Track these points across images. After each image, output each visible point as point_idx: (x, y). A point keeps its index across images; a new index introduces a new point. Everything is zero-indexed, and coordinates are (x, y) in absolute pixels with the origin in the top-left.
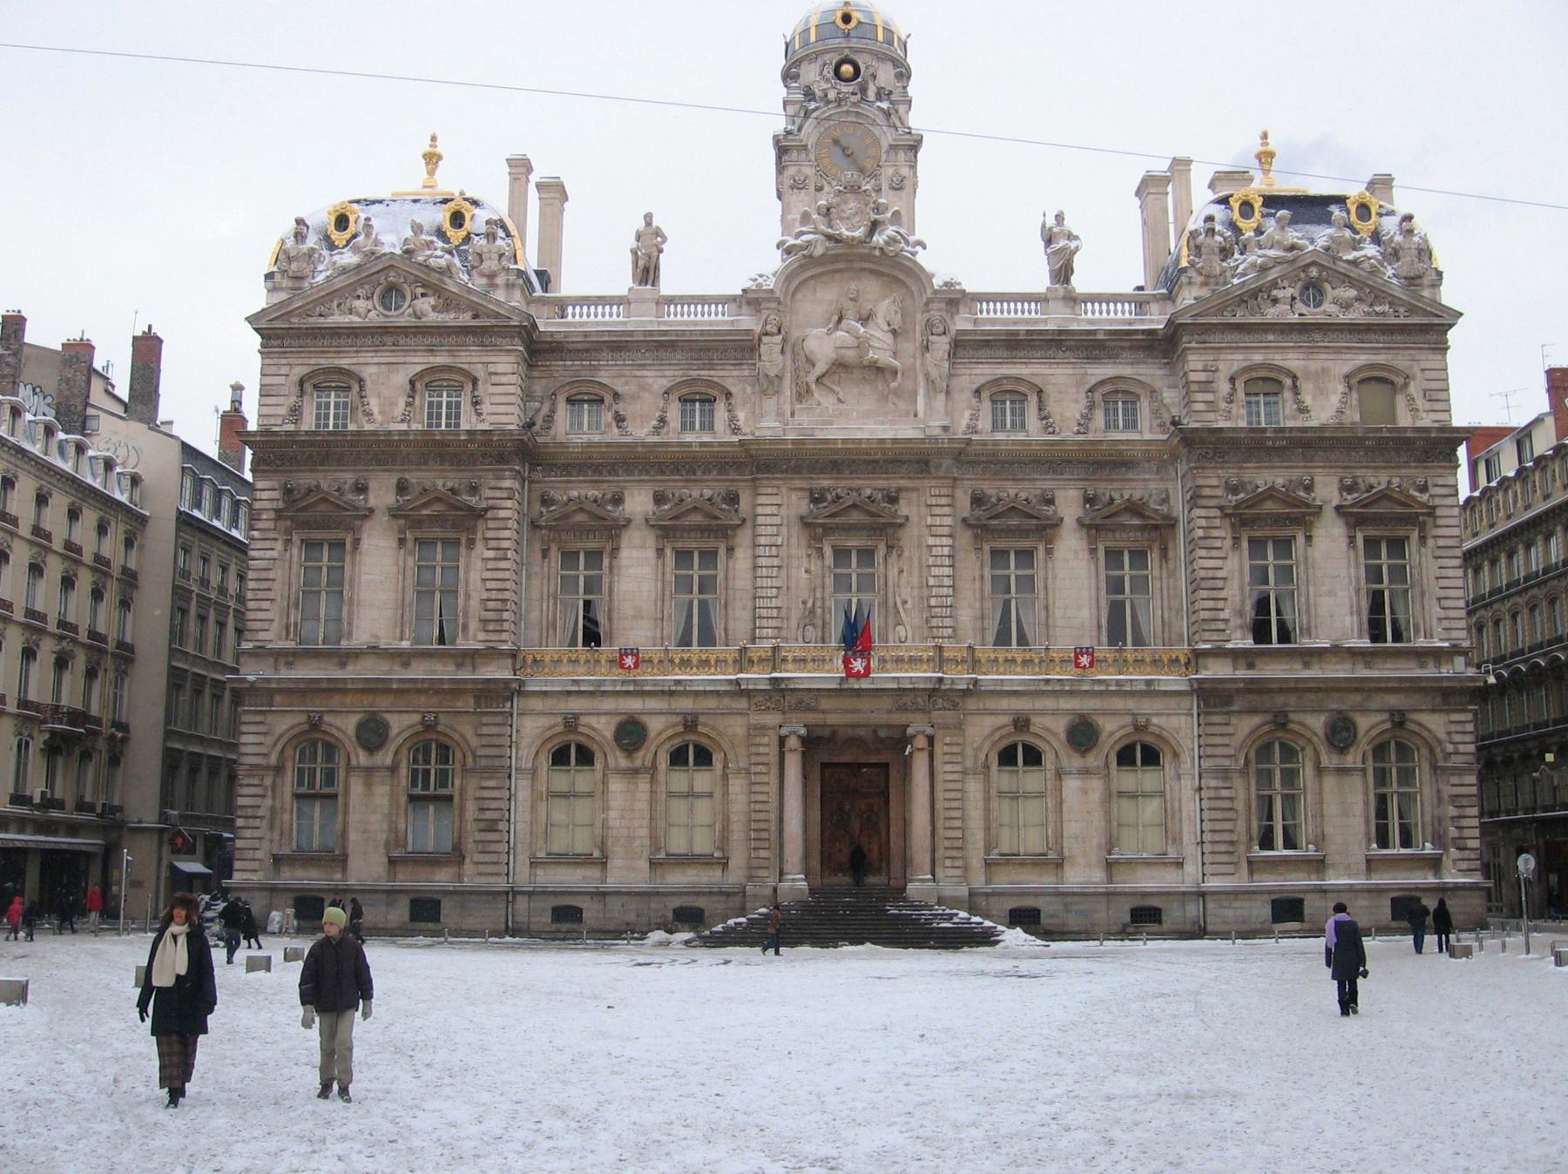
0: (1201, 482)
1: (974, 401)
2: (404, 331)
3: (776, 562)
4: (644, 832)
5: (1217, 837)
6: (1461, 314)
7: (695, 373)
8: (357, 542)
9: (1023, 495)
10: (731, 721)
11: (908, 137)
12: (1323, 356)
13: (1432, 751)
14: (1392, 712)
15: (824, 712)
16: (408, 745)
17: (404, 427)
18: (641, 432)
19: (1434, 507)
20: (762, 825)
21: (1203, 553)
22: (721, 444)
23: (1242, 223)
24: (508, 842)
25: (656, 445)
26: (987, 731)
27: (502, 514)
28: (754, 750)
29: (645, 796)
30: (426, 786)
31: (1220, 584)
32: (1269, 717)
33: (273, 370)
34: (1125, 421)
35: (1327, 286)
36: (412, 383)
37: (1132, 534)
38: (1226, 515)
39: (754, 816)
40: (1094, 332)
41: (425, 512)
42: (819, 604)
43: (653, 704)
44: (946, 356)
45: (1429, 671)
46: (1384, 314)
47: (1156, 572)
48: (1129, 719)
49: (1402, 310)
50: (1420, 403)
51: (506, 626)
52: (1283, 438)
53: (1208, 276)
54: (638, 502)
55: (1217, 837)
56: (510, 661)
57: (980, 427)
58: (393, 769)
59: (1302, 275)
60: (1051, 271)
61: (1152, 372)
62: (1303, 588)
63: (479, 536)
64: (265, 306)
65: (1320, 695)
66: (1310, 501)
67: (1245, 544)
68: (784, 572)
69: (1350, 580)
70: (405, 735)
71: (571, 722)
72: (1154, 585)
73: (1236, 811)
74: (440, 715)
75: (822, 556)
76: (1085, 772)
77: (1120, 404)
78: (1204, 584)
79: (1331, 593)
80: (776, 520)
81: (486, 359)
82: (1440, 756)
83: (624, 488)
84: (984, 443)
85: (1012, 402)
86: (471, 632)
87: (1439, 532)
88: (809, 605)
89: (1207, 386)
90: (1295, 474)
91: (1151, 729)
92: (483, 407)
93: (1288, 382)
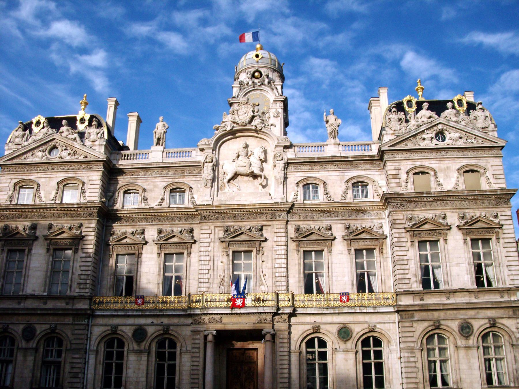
0: (395, 217)
1: (296, 188)
3: (208, 258)
4: (144, 379)
5: (409, 380)
7: (177, 180)
8: (30, 250)
9: (317, 227)
10: (184, 328)
11: (280, 97)
12: (447, 162)
13: (510, 336)
14: (489, 319)
15: (224, 324)
16: (44, 338)
17: (53, 202)
18: (154, 203)
19: (502, 225)
20: (196, 377)
21: (398, 249)
22: (185, 208)
24: (83, 383)
25: (158, 209)
26: (300, 333)
27: (90, 238)
28: (193, 341)
29: (145, 363)
30: (51, 357)
31: (406, 262)
32: (431, 323)
33: (4, 181)
34: (362, 195)
35: (446, 132)
36: (58, 184)
37: (366, 243)
38: (408, 231)
39: (192, 372)
40: (347, 157)
41: (58, 237)
42: (226, 276)
43: (149, 321)
44: (283, 169)
45: (506, 298)
47: (378, 259)
48: (366, 326)
49: (480, 141)
50: (492, 180)
51: (88, 286)
54: (151, 234)
55: (409, 380)
56: (88, 302)
57: (298, 199)
58: (36, 350)
62: (444, 264)
63: (80, 248)
65: (455, 312)
66: (445, 224)
67: (416, 244)
68: (211, 263)
69: (466, 258)
70: (42, 334)
71: (114, 329)
72: (377, 265)
73: (418, 368)
74: (58, 325)
75: (227, 253)
76: (346, 351)
77: (360, 187)
78: (399, 263)
79: (457, 264)
80: (209, 240)
81: (88, 175)
82: (514, 339)
83: (145, 228)
84: (299, 204)
85: (313, 188)
86: (73, 289)
87: (505, 236)
88: (222, 277)
89: (395, 176)
90: (438, 213)
91: (377, 330)
93: (432, 173)
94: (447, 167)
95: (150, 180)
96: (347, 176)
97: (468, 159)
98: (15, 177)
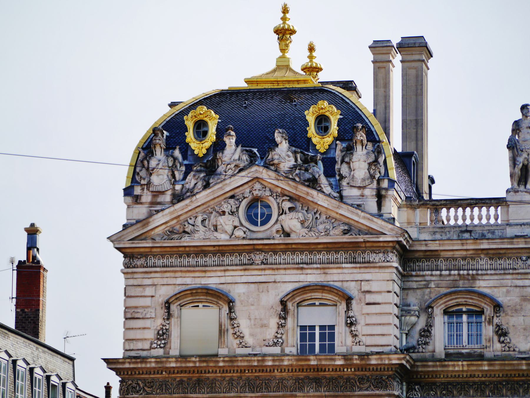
2: (274, 249)
17: (277, 350)
36: (283, 303)
64: (125, 222)
81: (359, 277)
92: (359, 327)
95: (509, 280)
98: (165, 281)
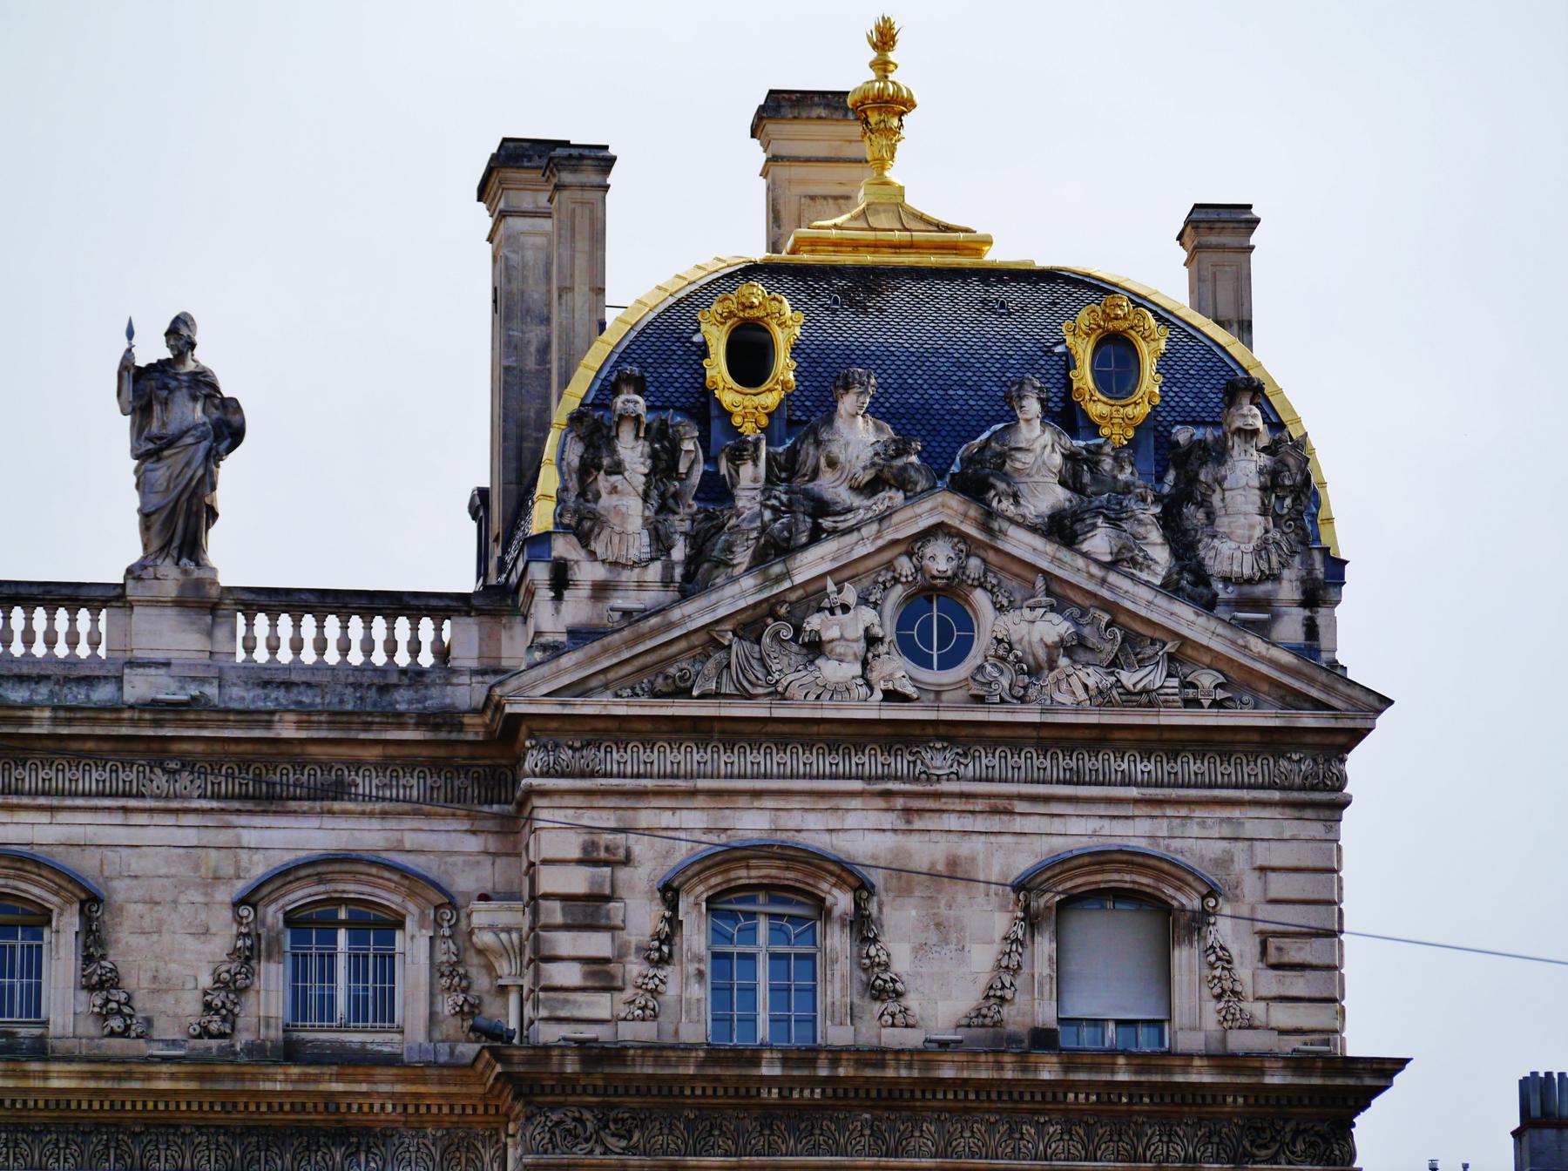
6: (1389, 702)
12: (952, 822)
23: (729, 394)
35: (980, 598)
40: (265, 717)
46: (1146, 698)
49: (1207, 680)
52: (814, 1081)
53: (615, 564)
59: (905, 566)
60: (146, 517)
61: (441, 842)
93: (842, 901)
94: (953, 862)
96: (258, 857)
97: (1102, 810)
